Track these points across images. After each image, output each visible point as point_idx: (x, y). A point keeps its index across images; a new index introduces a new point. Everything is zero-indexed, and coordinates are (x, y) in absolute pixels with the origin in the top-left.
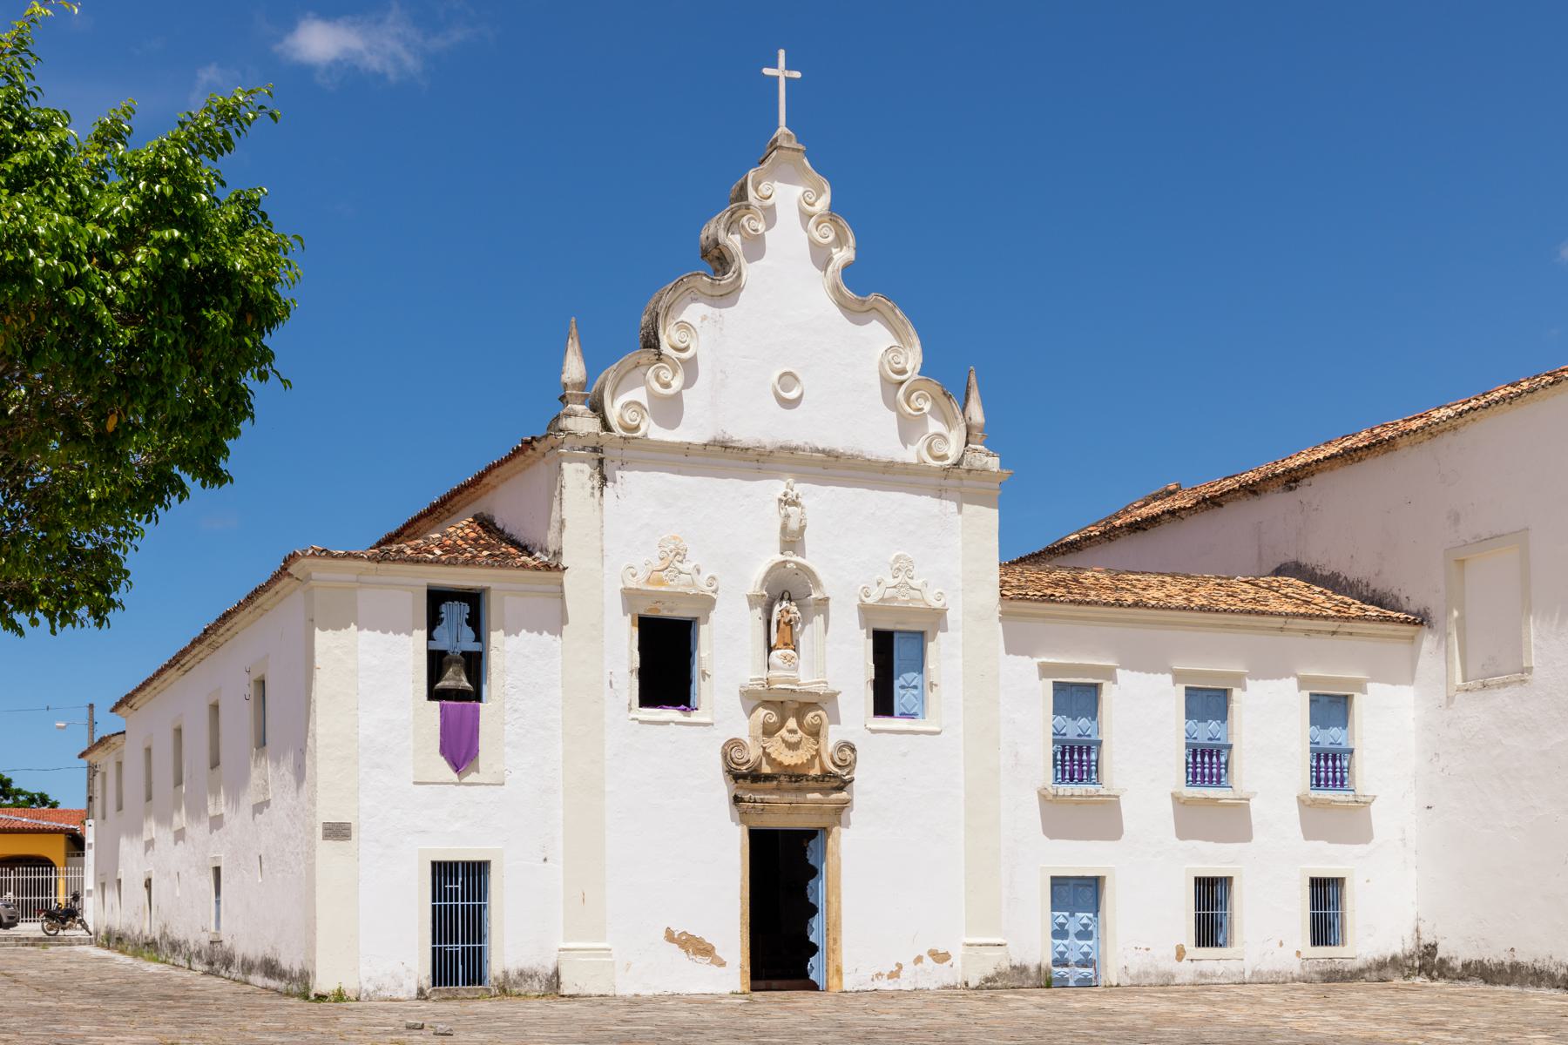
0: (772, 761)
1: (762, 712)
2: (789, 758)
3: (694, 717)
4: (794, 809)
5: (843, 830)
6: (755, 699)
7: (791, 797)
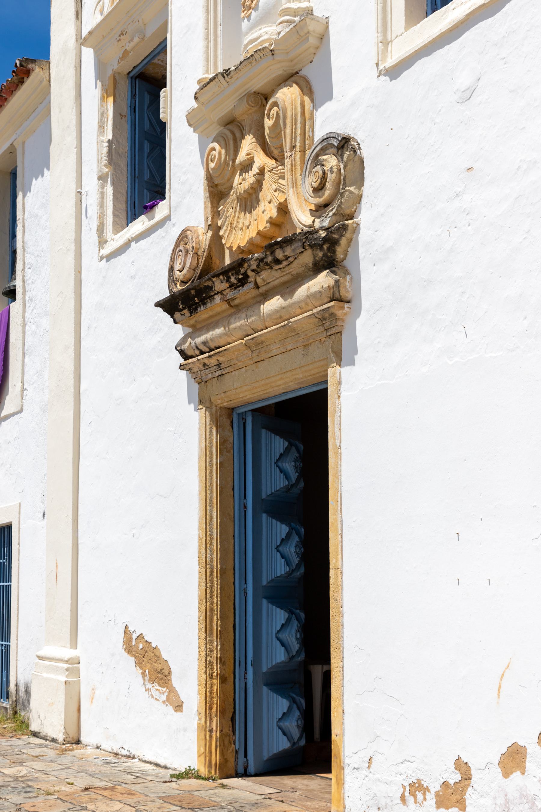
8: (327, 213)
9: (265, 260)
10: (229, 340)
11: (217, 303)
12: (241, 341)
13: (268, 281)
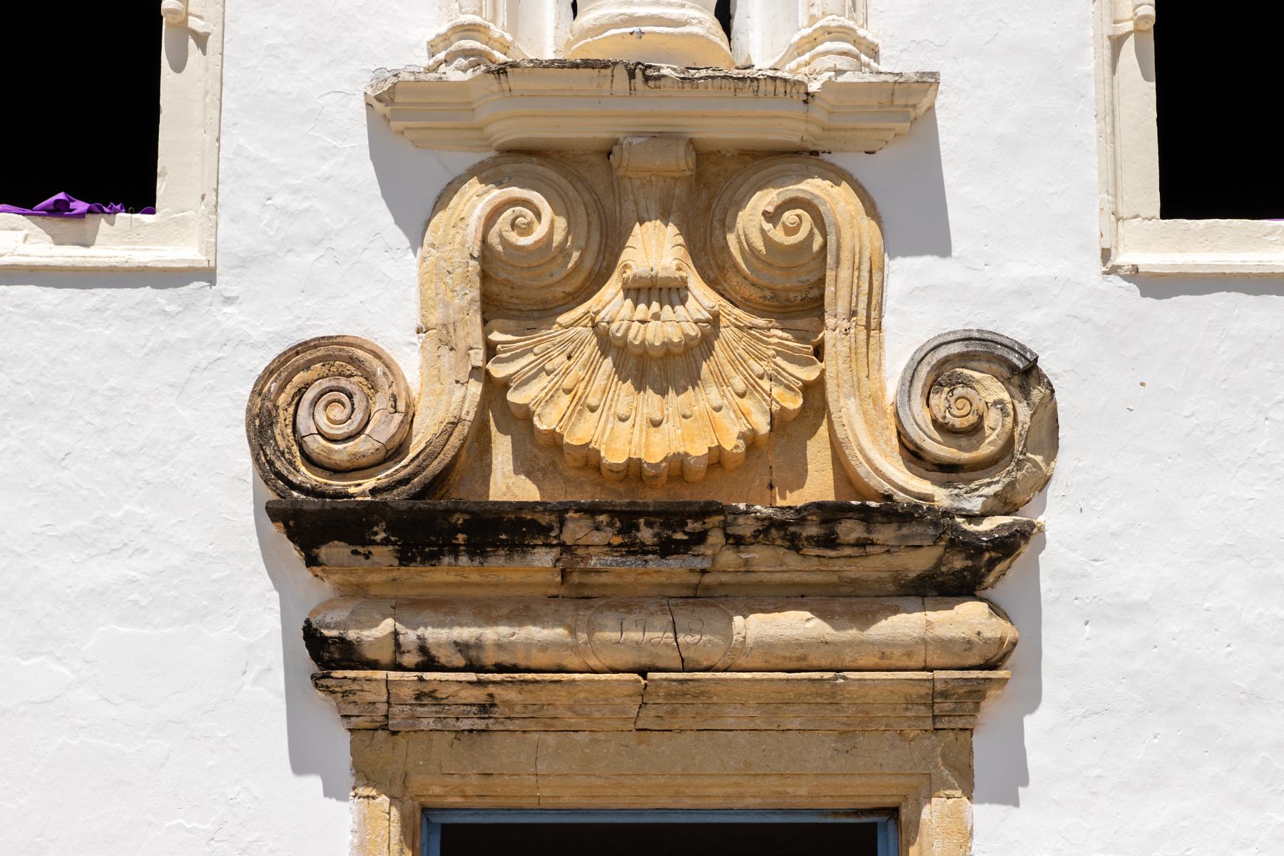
0: (541, 452)
1: (476, 200)
2: (634, 430)
3: (118, 238)
4: (668, 698)
5: (982, 815)
6: (434, 131)
7: (649, 636)
8: (973, 486)
9: (792, 529)
10: (572, 661)
11: (537, 564)
12: (636, 676)
13: (756, 569)
